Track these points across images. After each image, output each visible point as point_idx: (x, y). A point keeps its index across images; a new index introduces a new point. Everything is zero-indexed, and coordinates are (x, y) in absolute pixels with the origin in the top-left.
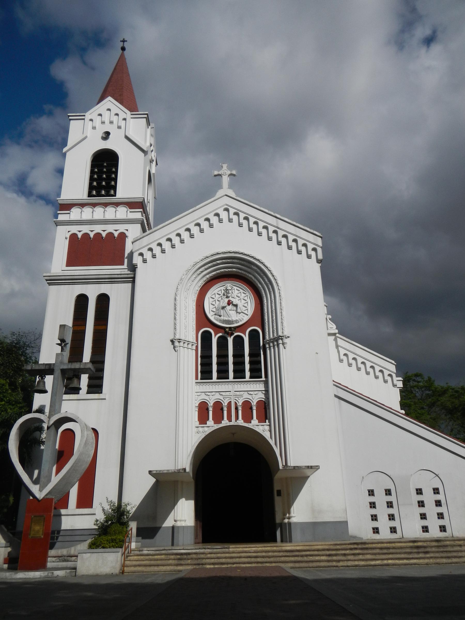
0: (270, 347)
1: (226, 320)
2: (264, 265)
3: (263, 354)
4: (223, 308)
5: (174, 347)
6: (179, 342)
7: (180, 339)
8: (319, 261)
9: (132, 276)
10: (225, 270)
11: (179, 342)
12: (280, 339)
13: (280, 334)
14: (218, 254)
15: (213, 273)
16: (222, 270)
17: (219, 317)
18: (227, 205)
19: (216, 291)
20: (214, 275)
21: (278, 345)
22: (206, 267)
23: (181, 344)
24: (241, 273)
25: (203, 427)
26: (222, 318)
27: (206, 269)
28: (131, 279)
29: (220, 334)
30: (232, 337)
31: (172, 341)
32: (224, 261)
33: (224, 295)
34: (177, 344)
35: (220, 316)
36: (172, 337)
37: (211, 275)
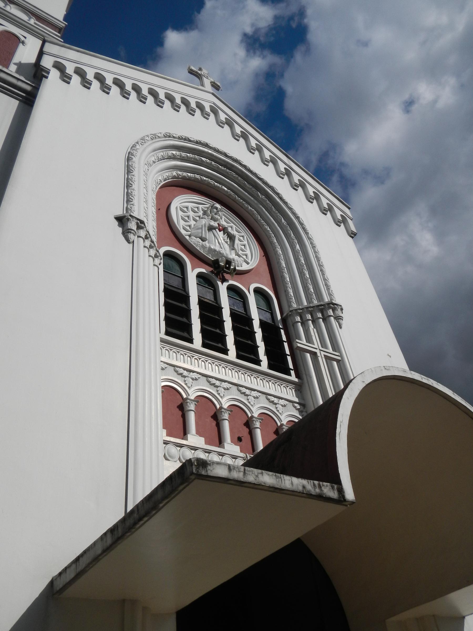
0: (304, 323)
1: (215, 250)
2: (281, 198)
3: (285, 334)
4: (211, 228)
5: (126, 233)
6: (139, 228)
7: (142, 222)
8: (352, 235)
9: (28, 88)
10: (210, 180)
11: (139, 228)
12: (330, 308)
13: (326, 299)
14: (206, 145)
15: (189, 174)
16: (205, 178)
17: (200, 241)
18: (214, 104)
19: (190, 205)
20: (189, 179)
21: (325, 319)
22: (184, 154)
23: (142, 233)
24: (234, 200)
25: (181, 446)
26: (206, 244)
27: (182, 159)
28: (24, 95)
29: (203, 270)
30: (226, 284)
31: (122, 220)
32: (213, 163)
33: (205, 213)
34: (132, 225)
35: (203, 239)
36: (120, 212)
37: (185, 174)
